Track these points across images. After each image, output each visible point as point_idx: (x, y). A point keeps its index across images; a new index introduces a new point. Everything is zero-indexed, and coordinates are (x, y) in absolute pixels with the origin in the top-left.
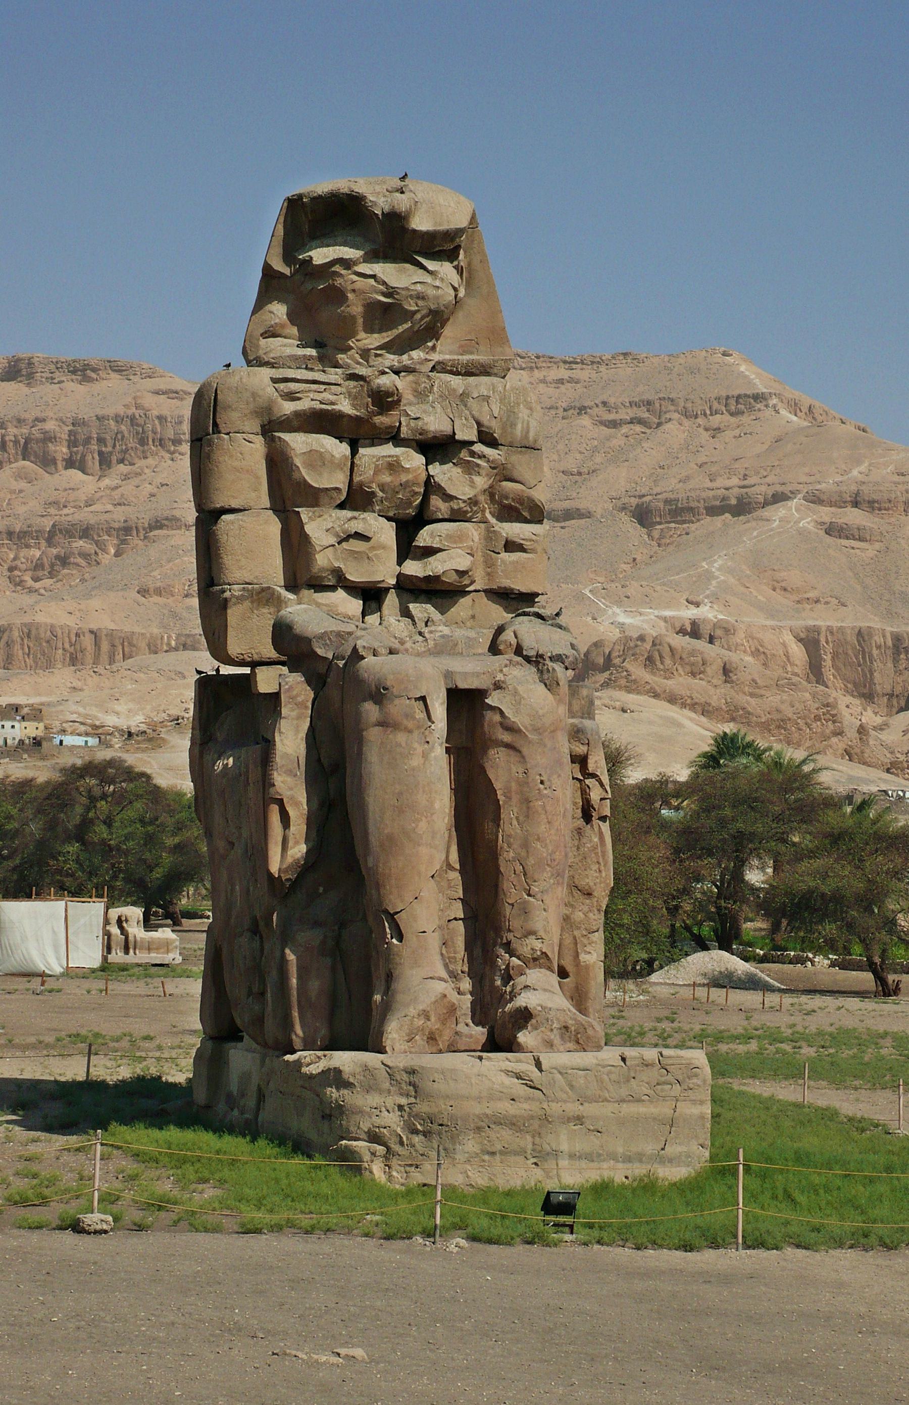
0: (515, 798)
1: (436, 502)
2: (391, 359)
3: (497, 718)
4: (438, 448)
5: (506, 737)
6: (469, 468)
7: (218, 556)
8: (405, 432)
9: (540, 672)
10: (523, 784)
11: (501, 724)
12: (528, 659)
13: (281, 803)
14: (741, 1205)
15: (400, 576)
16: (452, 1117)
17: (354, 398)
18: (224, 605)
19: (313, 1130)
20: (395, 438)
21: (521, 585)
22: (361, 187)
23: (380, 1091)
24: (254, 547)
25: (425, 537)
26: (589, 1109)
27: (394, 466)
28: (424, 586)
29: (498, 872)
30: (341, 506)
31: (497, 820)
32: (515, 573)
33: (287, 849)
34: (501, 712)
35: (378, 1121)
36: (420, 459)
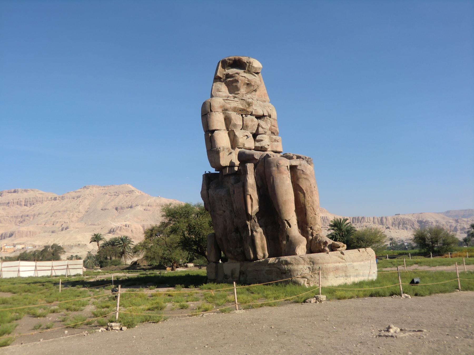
0: (309, 191)
1: (260, 129)
2: (249, 96)
3: (302, 172)
4: (258, 117)
6: (266, 121)
7: (214, 141)
8: (254, 113)
9: (307, 162)
10: (310, 187)
11: (303, 173)
12: (303, 159)
13: (250, 195)
14: (401, 283)
15: (255, 147)
16: (327, 269)
17: (242, 104)
18: (218, 152)
19: (280, 276)
20: (251, 114)
23: (301, 264)
25: (258, 137)
26: (355, 264)
28: (260, 149)
29: (306, 209)
30: (241, 129)
31: (305, 197)
33: (253, 207)
34: (302, 171)
35: (303, 272)
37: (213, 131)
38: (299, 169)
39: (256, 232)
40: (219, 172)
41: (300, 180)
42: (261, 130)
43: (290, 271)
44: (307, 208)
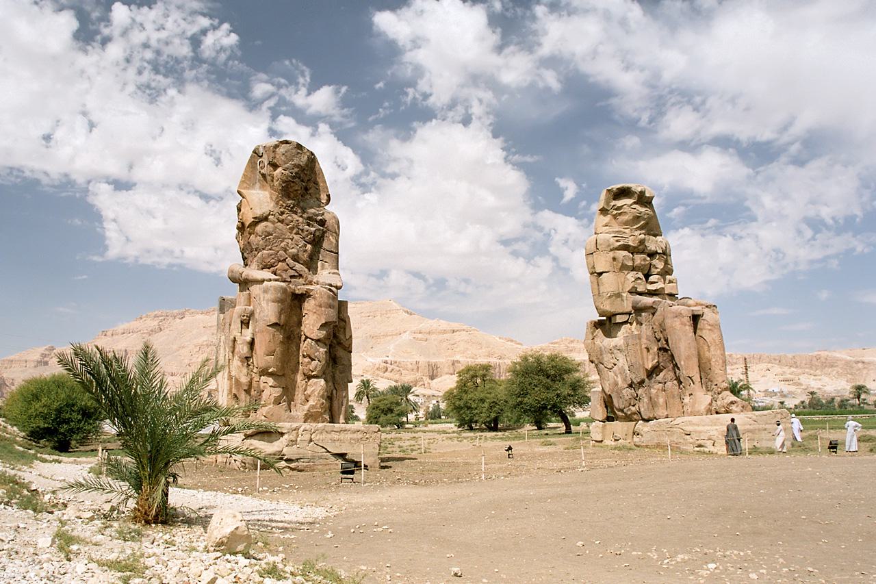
1: (653, 270)
2: (639, 232)
4: (652, 255)
5: (709, 328)
12: (707, 307)
20: (642, 252)
21: (674, 292)
22: (629, 185)
24: (610, 282)
25: (652, 279)
26: (767, 426)
27: (645, 260)
28: (653, 292)
31: (709, 350)
32: (669, 289)
36: (648, 259)
37: (600, 274)
38: (704, 320)
39: (653, 387)
40: (605, 318)
41: (704, 331)
42: (654, 271)
43: (695, 432)
44: (713, 364)
